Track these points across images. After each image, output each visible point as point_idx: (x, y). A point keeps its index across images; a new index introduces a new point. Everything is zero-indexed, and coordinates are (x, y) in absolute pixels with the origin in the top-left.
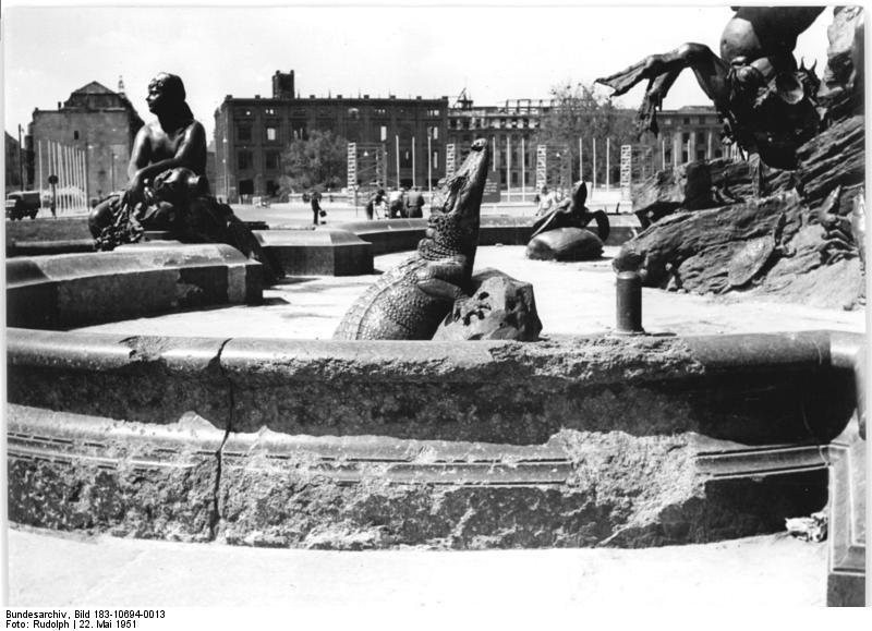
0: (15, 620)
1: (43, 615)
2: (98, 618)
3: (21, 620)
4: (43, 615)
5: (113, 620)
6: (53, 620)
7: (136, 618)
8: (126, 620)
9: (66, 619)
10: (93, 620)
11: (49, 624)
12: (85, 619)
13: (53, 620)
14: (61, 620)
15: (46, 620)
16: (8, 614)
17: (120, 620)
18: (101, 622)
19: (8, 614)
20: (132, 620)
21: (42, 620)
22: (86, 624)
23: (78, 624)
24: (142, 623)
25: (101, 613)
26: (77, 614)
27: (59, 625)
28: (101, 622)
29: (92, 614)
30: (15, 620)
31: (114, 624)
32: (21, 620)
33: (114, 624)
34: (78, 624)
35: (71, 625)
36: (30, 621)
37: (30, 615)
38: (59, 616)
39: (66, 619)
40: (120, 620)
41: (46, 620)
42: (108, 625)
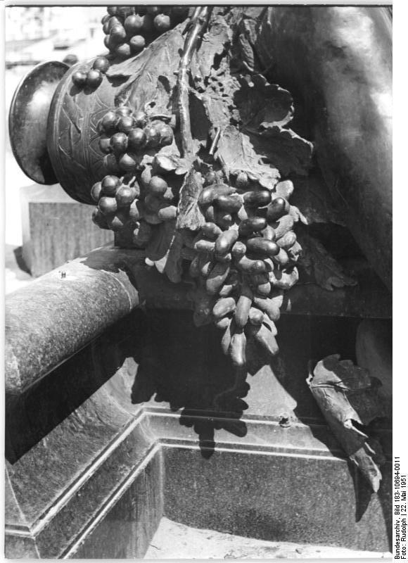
0: (401, 553)
1: (398, 536)
2: (400, 499)
3: (401, 550)
4: (398, 536)
5: (401, 490)
6: (401, 529)
7: (399, 475)
8: (400, 483)
9: (400, 520)
10: (401, 503)
11: (404, 531)
12: (400, 508)
13: (401, 529)
14: (401, 524)
15: (401, 533)
16: (397, 557)
17: (401, 485)
18: (402, 498)
19: (397, 557)
20: (401, 478)
21: (401, 536)
22: (403, 508)
23: (404, 513)
24: (401, 472)
25: (396, 498)
26: (397, 513)
27: (404, 525)
28: (402, 498)
29: (397, 503)
30: (401, 553)
31: (404, 489)
32: (401, 550)
33: (404, 489)
34: (404, 513)
35: (404, 517)
36: (401, 544)
37: (398, 543)
38: (398, 525)
39: (400, 520)
40: (401, 485)
41: (401, 533)
42: (404, 493)
